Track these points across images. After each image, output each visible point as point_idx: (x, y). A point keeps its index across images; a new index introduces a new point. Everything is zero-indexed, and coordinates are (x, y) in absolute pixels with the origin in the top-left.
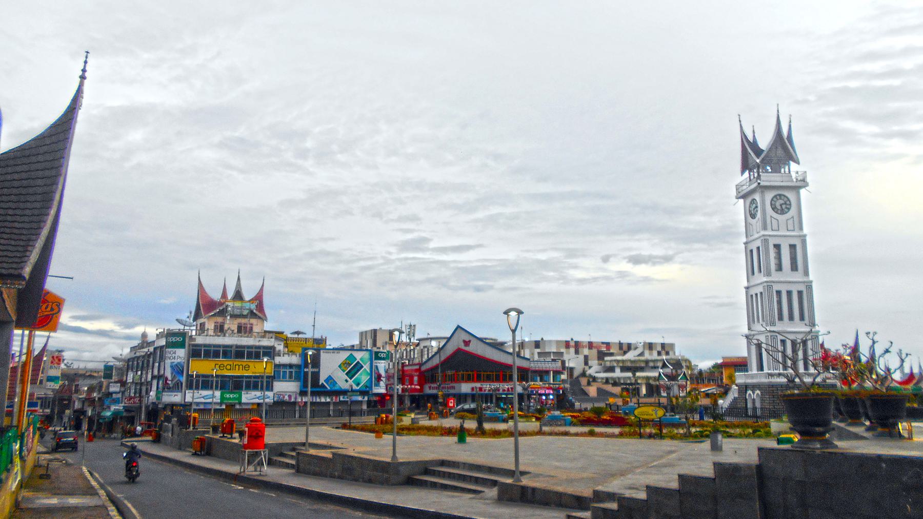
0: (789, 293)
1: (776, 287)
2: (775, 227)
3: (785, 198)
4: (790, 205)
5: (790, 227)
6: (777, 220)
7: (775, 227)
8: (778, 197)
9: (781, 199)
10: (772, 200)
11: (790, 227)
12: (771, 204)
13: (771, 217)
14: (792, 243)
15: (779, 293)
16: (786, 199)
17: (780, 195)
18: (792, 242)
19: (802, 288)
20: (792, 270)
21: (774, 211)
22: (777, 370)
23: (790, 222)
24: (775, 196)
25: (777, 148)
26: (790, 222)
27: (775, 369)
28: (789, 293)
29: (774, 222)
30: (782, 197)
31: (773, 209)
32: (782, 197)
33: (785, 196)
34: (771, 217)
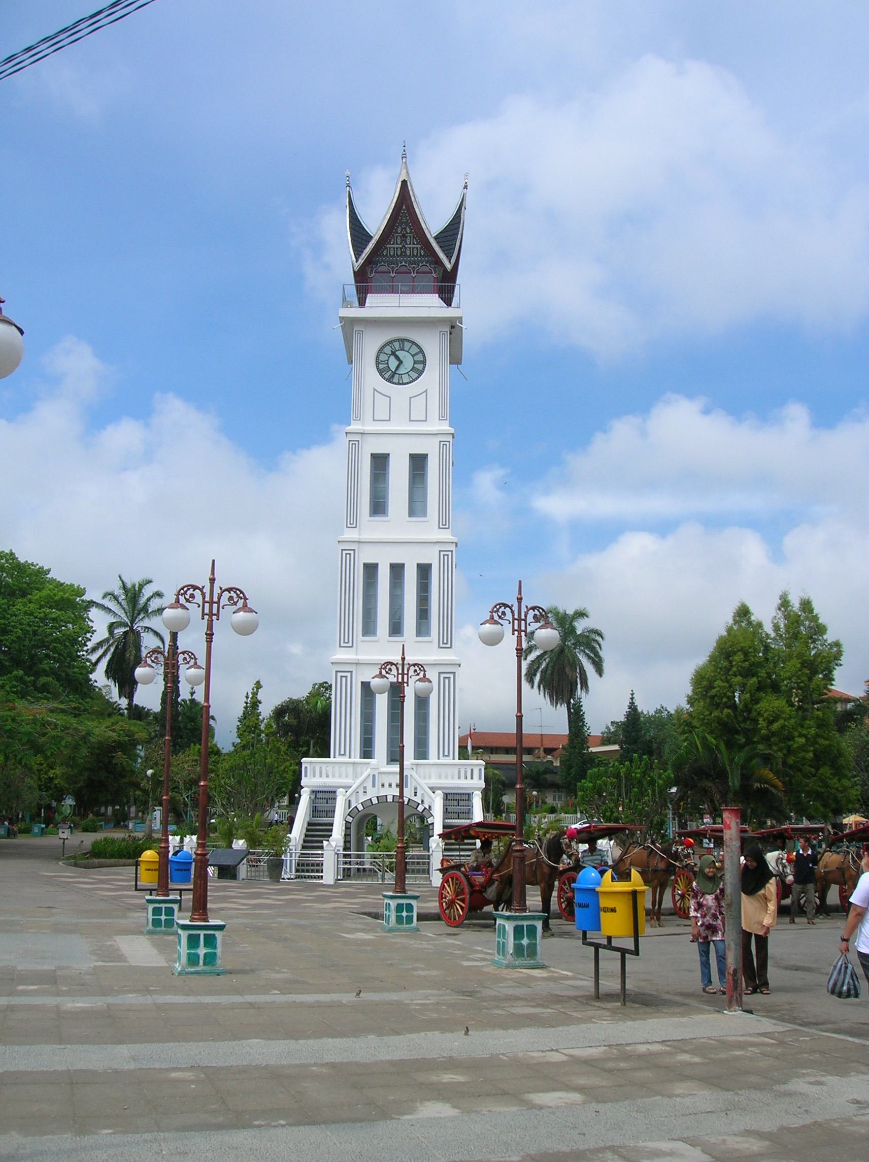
0: (397, 570)
1: (367, 556)
2: (382, 414)
4: (424, 362)
5: (418, 414)
6: (390, 397)
7: (382, 414)
8: (397, 345)
9: (403, 350)
10: (381, 351)
11: (418, 414)
12: (378, 363)
15: (371, 570)
16: (414, 350)
17: (402, 341)
19: (430, 556)
20: (412, 513)
22: (344, 755)
24: (390, 343)
27: (340, 754)
28: (397, 570)
30: (407, 345)
31: (381, 372)
32: (407, 345)
33: (413, 343)
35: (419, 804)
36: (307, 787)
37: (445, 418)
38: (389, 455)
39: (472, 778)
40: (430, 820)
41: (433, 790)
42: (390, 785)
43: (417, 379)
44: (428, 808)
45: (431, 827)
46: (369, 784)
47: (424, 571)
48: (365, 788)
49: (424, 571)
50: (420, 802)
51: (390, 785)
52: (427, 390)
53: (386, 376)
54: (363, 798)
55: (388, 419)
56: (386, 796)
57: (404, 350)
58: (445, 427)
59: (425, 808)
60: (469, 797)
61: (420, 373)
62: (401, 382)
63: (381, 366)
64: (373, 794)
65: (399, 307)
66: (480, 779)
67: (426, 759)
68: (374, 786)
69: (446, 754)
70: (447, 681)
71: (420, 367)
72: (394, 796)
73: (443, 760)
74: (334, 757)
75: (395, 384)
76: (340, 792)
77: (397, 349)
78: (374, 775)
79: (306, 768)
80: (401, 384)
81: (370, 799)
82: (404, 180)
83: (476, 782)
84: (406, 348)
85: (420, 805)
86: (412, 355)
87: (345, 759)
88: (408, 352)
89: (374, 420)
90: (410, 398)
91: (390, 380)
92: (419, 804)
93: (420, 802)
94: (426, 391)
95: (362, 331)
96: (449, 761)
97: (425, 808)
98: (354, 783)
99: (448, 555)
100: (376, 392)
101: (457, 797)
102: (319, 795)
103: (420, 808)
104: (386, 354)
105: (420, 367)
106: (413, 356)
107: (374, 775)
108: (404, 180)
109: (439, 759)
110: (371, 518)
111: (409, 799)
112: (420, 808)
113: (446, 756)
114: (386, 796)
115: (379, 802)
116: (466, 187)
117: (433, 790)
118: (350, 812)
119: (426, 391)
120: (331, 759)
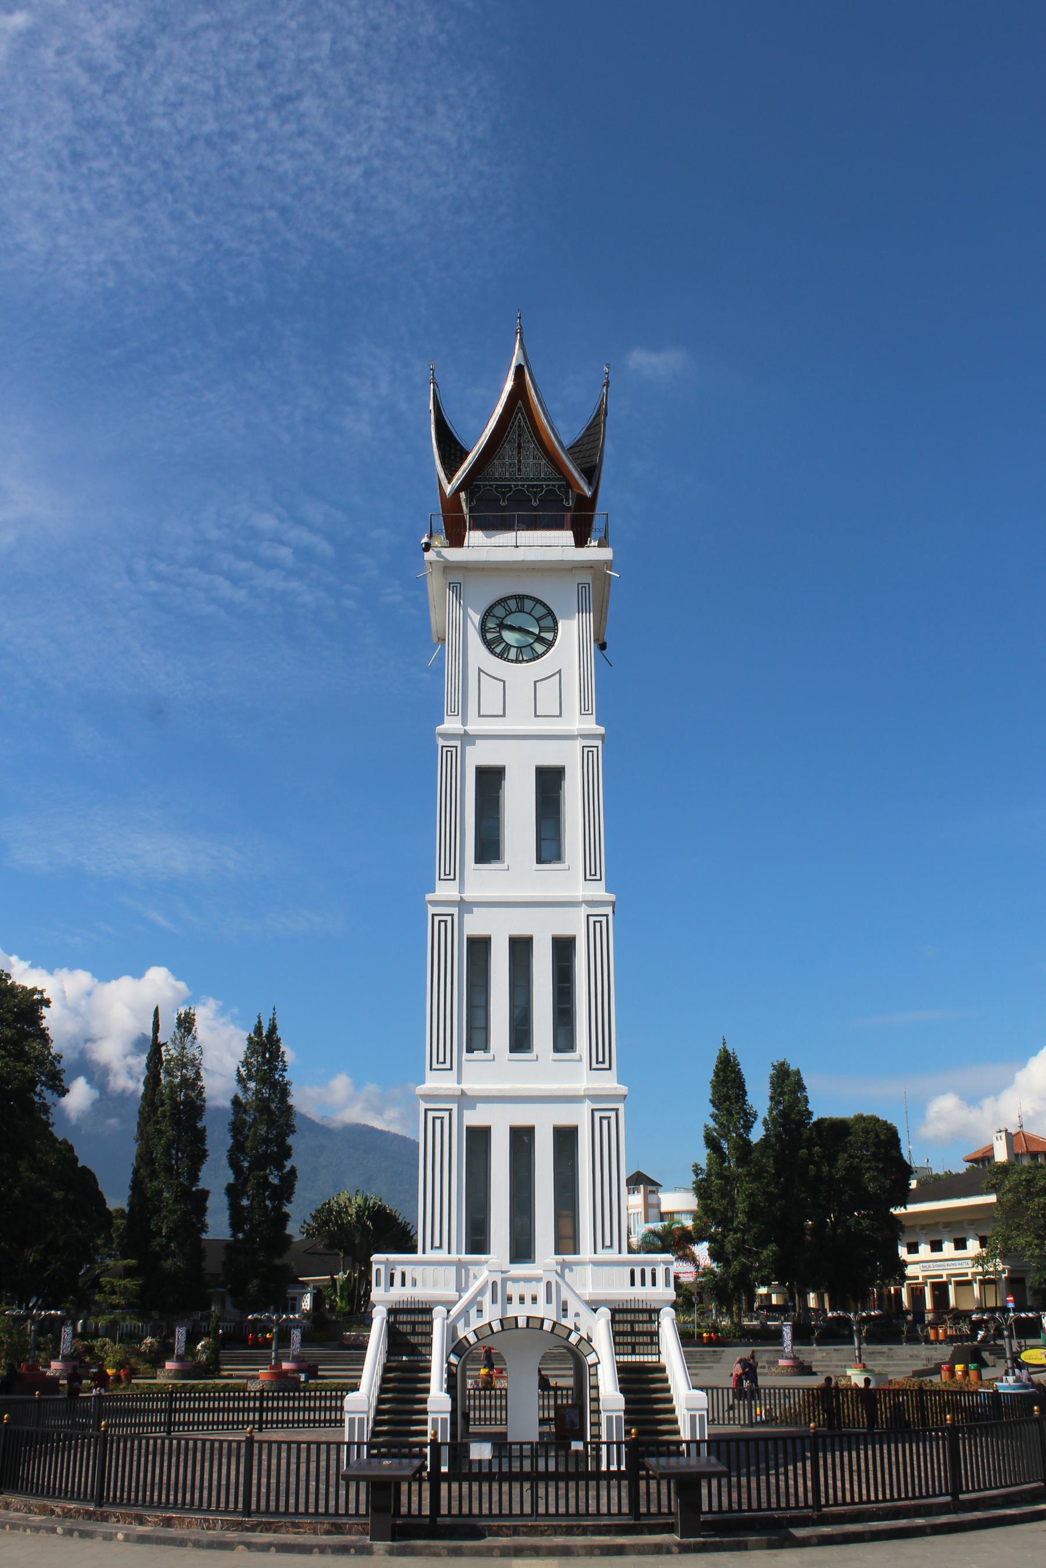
2: (492, 703)
3: (538, 606)
5: (548, 704)
6: (504, 682)
8: (512, 604)
9: (521, 610)
11: (548, 704)
12: (483, 630)
13: (480, 670)
14: (550, 761)
15: (479, 947)
16: (540, 611)
17: (520, 598)
18: (550, 756)
19: (574, 924)
21: (492, 652)
23: (548, 691)
25: (519, 447)
26: (548, 691)
29: (491, 691)
30: (528, 605)
31: (489, 645)
34: (480, 670)
35: (571, 1331)
36: (381, 1302)
37: (590, 712)
38: (504, 768)
39: (654, 1284)
40: (591, 1359)
41: (594, 1306)
42: (522, 1299)
43: (544, 654)
44: (586, 1338)
45: (593, 1370)
46: (487, 1298)
47: (563, 948)
48: (481, 1303)
49: (563, 948)
50: (573, 1328)
51: (522, 1299)
52: (560, 670)
53: (498, 650)
54: (476, 1323)
55: (502, 714)
56: (516, 1318)
57: (523, 612)
58: (590, 725)
59: (581, 1338)
60: (652, 1313)
61: (550, 644)
62: (521, 659)
63: (489, 636)
64: (492, 1314)
65: (517, 547)
66: (667, 1284)
67: (575, 1253)
68: (494, 1300)
69: (608, 1243)
70: (605, 1122)
71: (549, 636)
72: (528, 1318)
73: (604, 1255)
74: (424, 1252)
75: (512, 661)
76: (439, 1312)
77: (513, 611)
78: (494, 1283)
79: (378, 1270)
80: (520, 662)
81: (490, 1324)
82: (520, 364)
83: (661, 1291)
84: (527, 608)
85: (573, 1332)
86: (536, 619)
87: (442, 1255)
88: (530, 614)
89: (480, 716)
90: (535, 682)
91: (500, 656)
92: (571, 1331)
93: (573, 1328)
94: (560, 672)
95: (460, 584)
96: (612, 1255)
97: (581, 1338)
98: (460, 1298)
99: (601, 922)
100: (481, 673)
101: (629, 1317)
102: (402, 1318)
103: (574, 1339)
104: (494, 616)
105: (549, 636)
106: (538, 620)
107: (494, 1283)
108: (520, 364)
109: (595, 1252)
110: (479, 866)
111: (555, 1324)
112: (574, 1339)
113: (608, 1247)
114: (516, 1318)
115: (503, 1329)
116: (607, 384)
117: (594, 1306)
118: (454, 1347)
119: (560, 672)
120: (419, 1256)
